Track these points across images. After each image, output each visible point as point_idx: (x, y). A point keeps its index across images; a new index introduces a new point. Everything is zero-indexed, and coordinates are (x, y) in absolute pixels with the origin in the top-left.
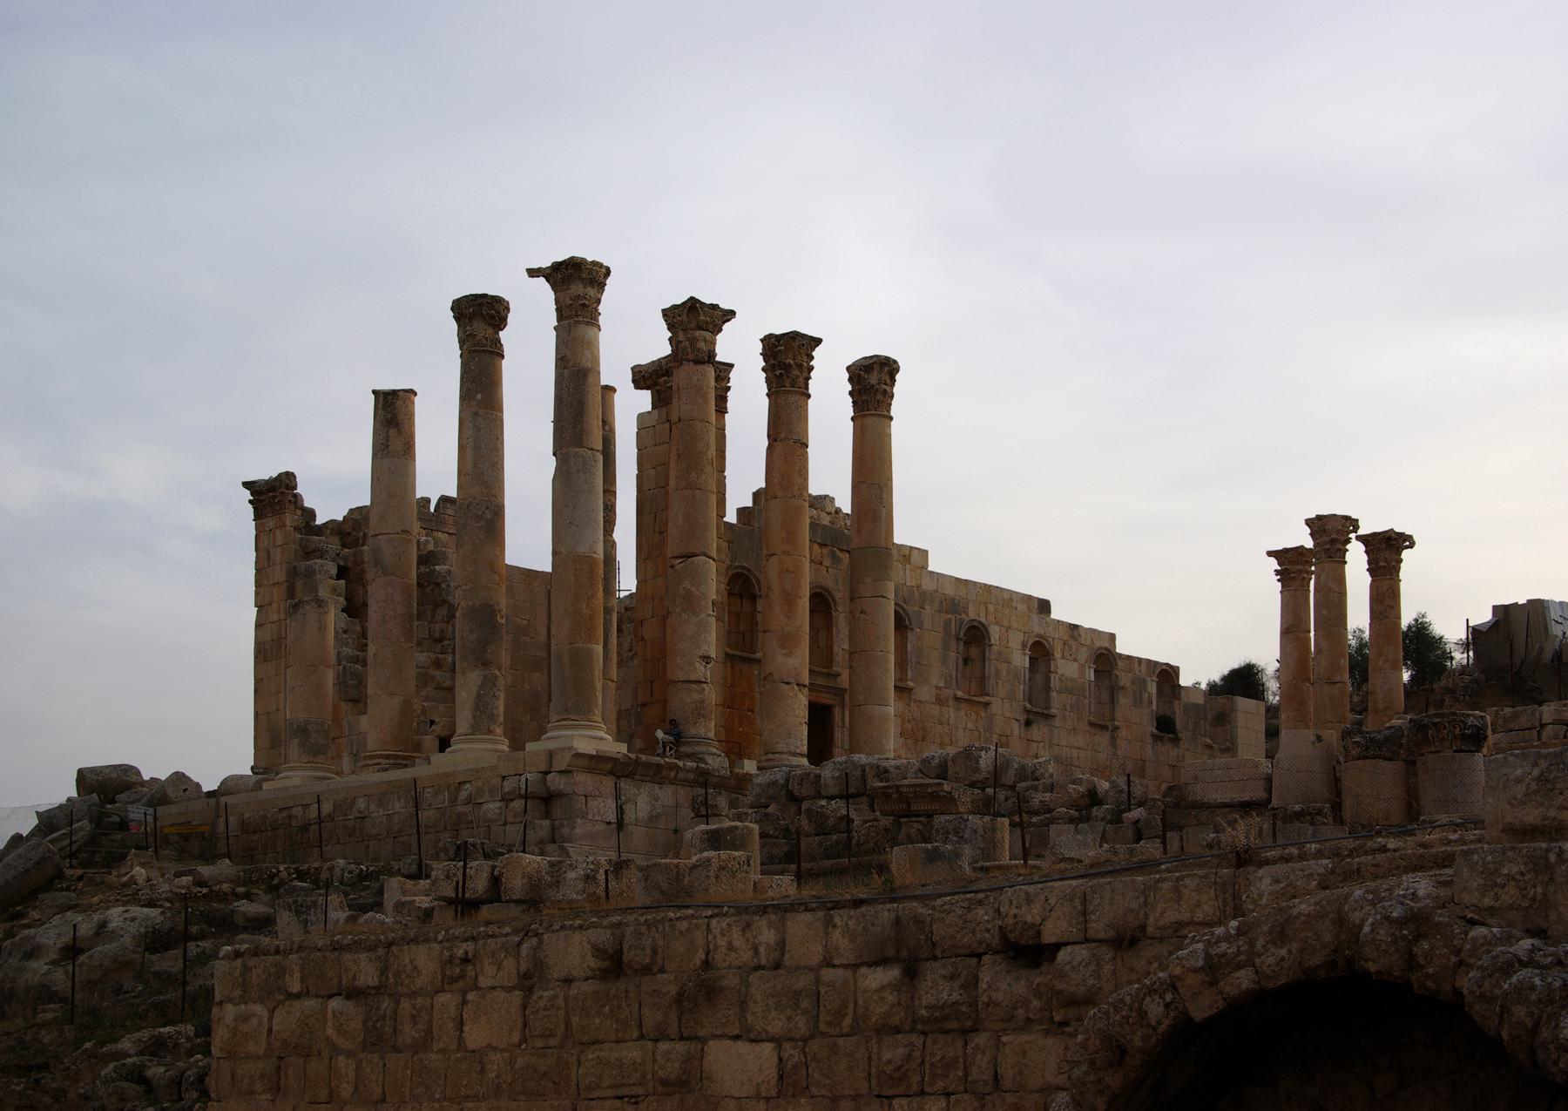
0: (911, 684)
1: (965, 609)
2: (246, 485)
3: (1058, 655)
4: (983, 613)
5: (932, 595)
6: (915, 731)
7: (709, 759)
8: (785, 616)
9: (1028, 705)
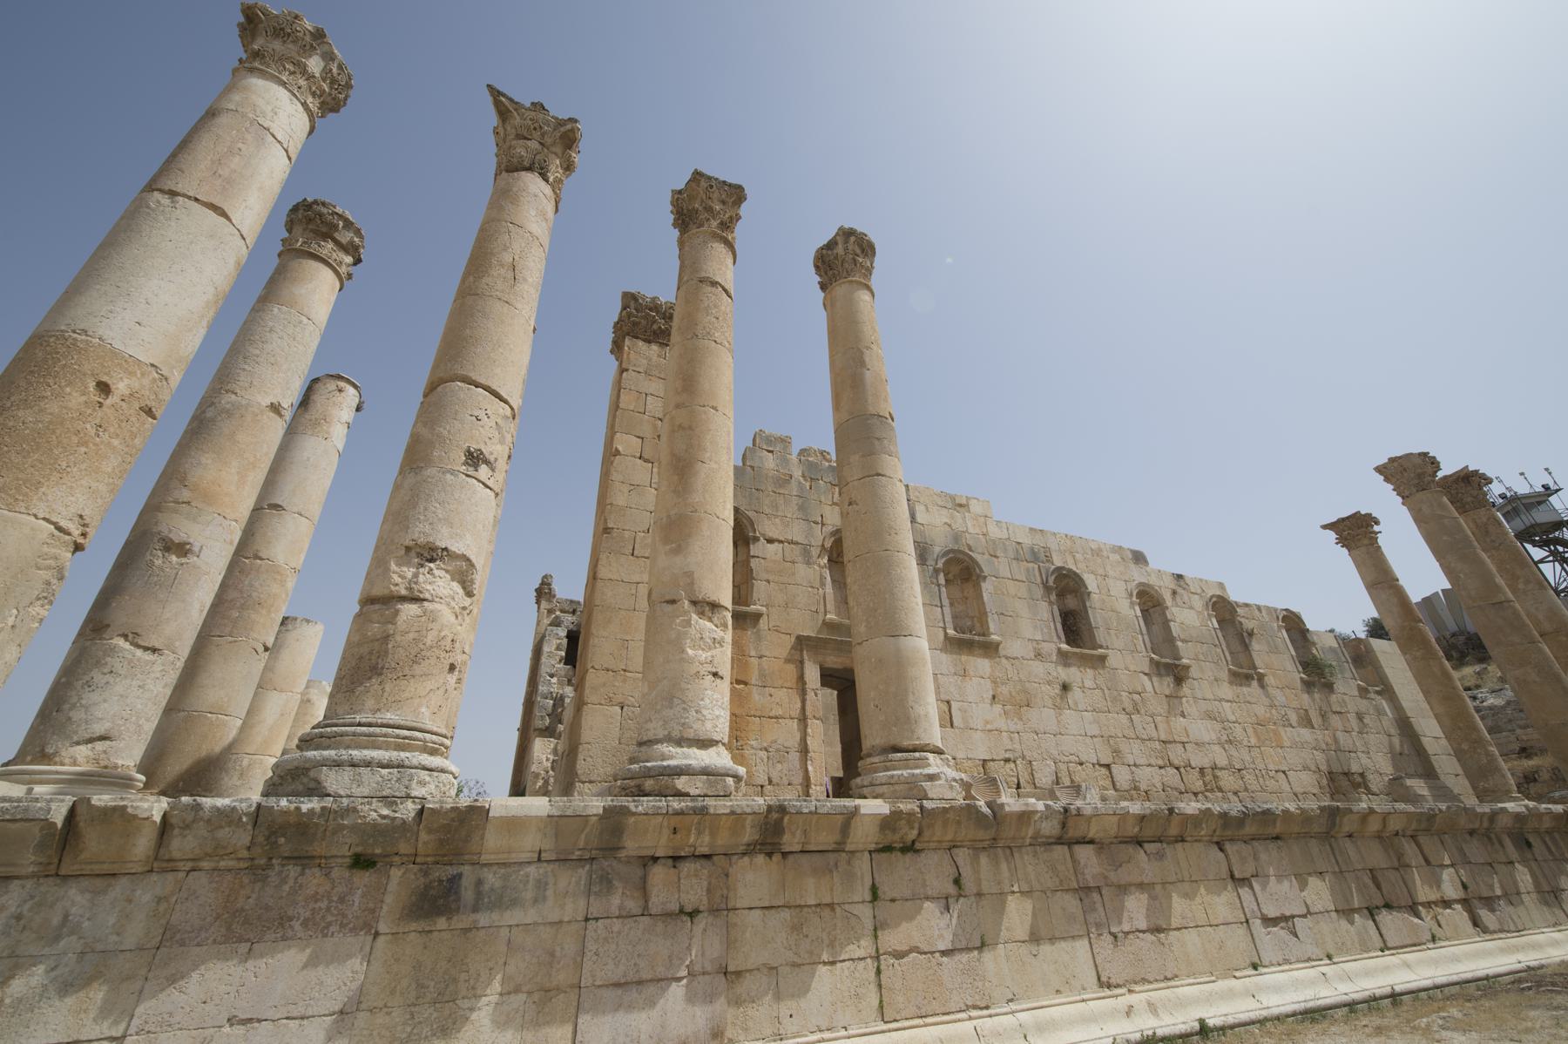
0: (995, 637)
1: (1049, 560)
6: (1014, 694)
7: (335, 781)
8: (674, 492)
9: (1153, 656)
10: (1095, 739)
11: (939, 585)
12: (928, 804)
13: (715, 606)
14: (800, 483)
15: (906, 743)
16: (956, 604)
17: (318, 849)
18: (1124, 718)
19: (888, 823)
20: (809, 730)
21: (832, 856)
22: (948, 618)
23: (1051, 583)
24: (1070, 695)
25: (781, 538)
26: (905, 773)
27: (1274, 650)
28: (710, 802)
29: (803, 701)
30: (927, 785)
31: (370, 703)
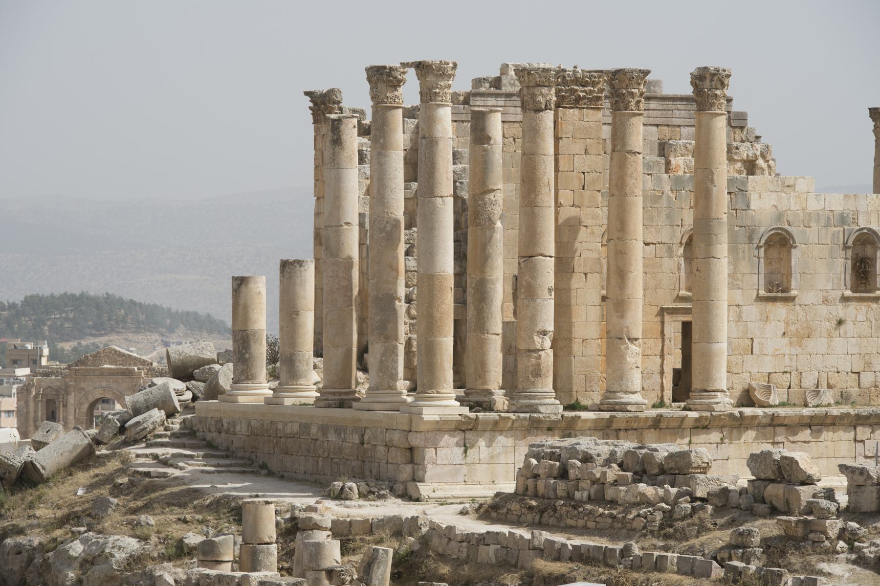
0: (794, 293)
5: (818, 215)
7: (542, 409)
8: (619, 287)
10: (853, 356)
11: (759, 258)
12: (714, 413)
13: (636, 339)
14: (669, 197)
15: (709, 389)
16: (774, 263)
17: (541, 426)
19: (697, 420)
20: (665, 362)
21: (676, 430)
22: (762, 282)
23: (850, 243)
24: (842, 327)
25: (655, 242)
26: (707, 401)
28: (638, 414)
29: (663, 346)
30: (715, 406)
31: (540, 386)
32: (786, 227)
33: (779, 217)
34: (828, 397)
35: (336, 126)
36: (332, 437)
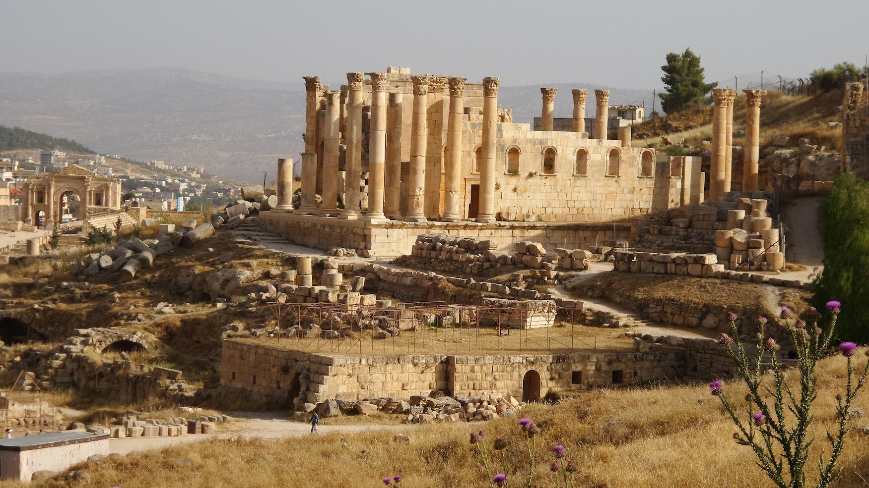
1: (546, 143)
2: (303, 78)
3: (591, 152)
4: (554, 142)
7: (419, 220)
18: (556, 194)
27: (632, 165)
32: (518, 145)
33: (515, 141)
34: (533, 218)
35: (314, 90)
36: (327, 229)
